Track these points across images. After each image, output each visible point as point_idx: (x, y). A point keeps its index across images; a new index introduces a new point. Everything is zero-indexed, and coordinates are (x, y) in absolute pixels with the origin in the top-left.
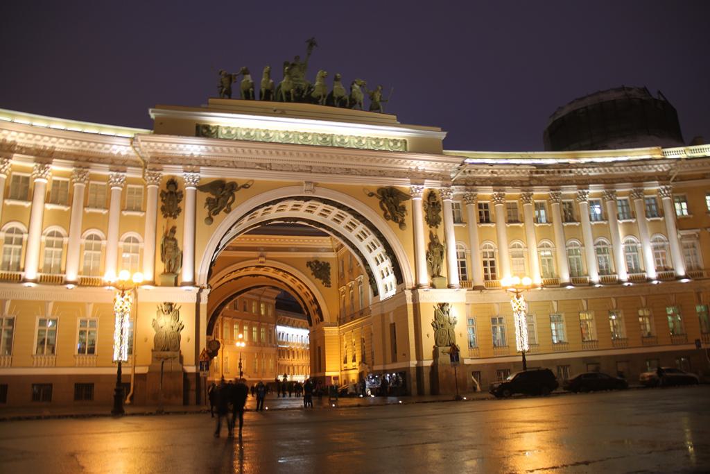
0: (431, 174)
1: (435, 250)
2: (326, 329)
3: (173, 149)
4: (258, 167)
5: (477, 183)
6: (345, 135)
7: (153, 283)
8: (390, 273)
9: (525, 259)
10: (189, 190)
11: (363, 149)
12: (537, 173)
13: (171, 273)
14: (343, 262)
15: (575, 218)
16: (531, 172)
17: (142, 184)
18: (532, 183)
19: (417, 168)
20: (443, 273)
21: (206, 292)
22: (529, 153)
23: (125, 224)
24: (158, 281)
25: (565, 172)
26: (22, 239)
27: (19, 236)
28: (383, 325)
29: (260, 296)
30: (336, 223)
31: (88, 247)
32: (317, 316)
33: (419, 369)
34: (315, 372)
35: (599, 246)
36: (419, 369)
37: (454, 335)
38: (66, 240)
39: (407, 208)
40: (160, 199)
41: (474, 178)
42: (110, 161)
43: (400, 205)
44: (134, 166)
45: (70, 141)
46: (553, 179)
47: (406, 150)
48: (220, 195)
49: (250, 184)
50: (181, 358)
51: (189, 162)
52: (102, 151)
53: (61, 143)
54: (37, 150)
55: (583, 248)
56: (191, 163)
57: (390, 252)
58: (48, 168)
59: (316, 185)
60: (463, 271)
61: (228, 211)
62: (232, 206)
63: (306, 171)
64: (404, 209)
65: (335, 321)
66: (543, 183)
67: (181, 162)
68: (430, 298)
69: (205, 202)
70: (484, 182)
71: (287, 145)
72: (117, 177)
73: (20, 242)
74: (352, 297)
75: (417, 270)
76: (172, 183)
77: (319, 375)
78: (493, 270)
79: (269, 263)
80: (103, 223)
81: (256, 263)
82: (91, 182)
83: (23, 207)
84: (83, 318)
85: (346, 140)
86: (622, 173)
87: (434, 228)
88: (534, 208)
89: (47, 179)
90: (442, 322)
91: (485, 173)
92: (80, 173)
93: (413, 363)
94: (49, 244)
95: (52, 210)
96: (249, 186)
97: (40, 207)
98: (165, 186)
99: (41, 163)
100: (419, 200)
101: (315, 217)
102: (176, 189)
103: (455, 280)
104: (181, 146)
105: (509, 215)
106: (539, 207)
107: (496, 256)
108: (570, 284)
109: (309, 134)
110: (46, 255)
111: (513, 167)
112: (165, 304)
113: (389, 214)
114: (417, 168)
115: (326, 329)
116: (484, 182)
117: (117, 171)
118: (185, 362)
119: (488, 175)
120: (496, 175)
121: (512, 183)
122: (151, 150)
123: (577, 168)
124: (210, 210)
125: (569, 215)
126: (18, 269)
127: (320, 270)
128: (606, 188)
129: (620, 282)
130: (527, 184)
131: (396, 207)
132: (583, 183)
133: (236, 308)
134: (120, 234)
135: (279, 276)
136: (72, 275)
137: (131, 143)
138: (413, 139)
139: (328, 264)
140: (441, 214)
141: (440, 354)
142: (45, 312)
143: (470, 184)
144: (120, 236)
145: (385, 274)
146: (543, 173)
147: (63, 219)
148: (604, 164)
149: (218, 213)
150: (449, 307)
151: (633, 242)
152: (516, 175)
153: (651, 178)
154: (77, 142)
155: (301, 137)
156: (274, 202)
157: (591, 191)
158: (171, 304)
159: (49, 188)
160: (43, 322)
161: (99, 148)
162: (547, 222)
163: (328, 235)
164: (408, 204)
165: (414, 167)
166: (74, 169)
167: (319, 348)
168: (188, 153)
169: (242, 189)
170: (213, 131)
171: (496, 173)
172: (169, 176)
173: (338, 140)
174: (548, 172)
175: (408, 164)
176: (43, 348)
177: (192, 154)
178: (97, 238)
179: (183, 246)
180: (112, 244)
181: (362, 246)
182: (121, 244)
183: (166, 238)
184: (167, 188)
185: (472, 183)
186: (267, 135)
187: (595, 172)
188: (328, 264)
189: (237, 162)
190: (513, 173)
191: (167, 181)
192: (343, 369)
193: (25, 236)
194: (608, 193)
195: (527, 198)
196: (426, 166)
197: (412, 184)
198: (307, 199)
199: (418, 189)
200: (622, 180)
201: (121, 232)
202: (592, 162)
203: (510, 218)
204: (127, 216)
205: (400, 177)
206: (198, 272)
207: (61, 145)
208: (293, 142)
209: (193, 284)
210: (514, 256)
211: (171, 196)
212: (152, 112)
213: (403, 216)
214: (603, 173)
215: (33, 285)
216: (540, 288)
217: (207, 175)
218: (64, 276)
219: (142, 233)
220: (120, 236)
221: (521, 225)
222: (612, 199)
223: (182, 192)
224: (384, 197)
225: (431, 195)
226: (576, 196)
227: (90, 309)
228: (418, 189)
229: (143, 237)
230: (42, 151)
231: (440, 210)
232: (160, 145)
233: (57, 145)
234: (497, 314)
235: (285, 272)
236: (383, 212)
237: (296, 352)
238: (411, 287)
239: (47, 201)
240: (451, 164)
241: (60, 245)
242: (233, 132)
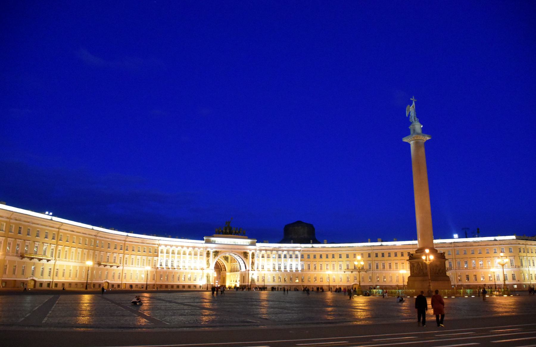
48: (216, 253)
56: (212, 248)
68: (251, 272)
70: (263, 250)
75: (249, 267)
76: (208, 251)
116: (263, 250)
121: (269, 250)
125: (280, 257)
132: (283, 251)
143: (261, 250)
200: (291, 251)
211: (208, 254)
217: (214, 250)
225: (253, 253)
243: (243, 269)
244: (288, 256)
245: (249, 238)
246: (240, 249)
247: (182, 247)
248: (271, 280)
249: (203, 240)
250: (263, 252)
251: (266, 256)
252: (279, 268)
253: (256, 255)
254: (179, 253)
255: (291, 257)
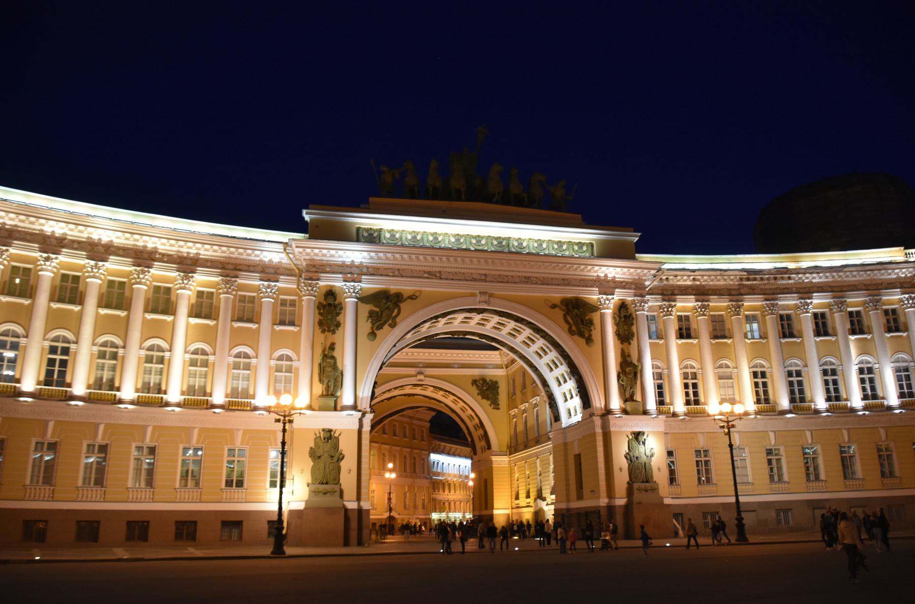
0: (622, 282)
1: (628, 370)
2: (494, 458)
3: (332, 256)
4: (426, 275)
5: (676, 292)
6: (523, 238)
7: (310, 408)
8: (574, 395)
9: (735, 381)
10: (350, 301)
11: (545, 255)
12: (748, 279)
13: (329, 397)
14: (514, 380)
15: (795, 333)
16: (741, 279)
17: (296, 294)
18: (742, 291)
19: (606, 276)
20: (638, 397)
21: (369, 417)
22: (738, 256)
23: (277, 341)
24: (315, 406)
25: (782, 278)
26: (163, 357)
27: (161, 354)
28: (566, 455)
29: (411, 418)
30: (511, 338)
31: (236, 366)
32: (483, 443)
33: (610, 508)
34: (480, 510)
35: (826, 367)
36: (610, 508)
37: (651, 469)
38: (211, 358)
39: (595, 322)
40: (317, 311)
41: (672, 286)
42: (260, 269)
43: (587, 318)
44: (288, 275)
45: (216, 248)
46: (767, 287)
47: (592, 254)
48: (384, 308)
49: (417, 294)
50: (341, 492)
51: (348, 270)
52: (253, 258)
53: (206, 250)
54: (180, 257)
55: (806, 369)
56: (351, 272)
57: (574, 371)
58: (192, 277)
59: (491, 295)
60: (661, 394)
61: (393, 326)
62: (398, 320)
63: (481, 280)
64: (591, 322)
65: (505, 449)
66: (756, 291)
67: (340, 270)
68: (623, 426)
69: (367, 314)
70: (685, 291)
71: (460, 251)
72: (269, 287)
73: (161, 360)
74: (526, 422)
76: (331, 293)
77: (484, 513)
78: (696, 394)
79: (428, 381)
80: (253, 339)
81: (413, 381)
82: (240, 293)
83: (165, 320)
84: (232, 447)
85: (525, 244)
86: (854, 279)
87: (626, 344)
88: (744, 321)
89: (190, 290)
90: (636, 454)
91: (685, 281)
92: (227, 282)
93: (603, 501)
94: (193, 363)
95: (197, 325)
96: (417, 297)
97: (183, 322)
98: (323, 297)
99: (184, 272)
100: (608, 312)
101: (488, 329)
102: (335, 300)
103: (651, 405)
104: (340, 252)
105: (714, 330)
106: (750, 319)
107: (699, 376)
108: (790, 412)
109: (483, 237)
110: (190, 375)
111: (719, 273)
112: (324, 430)
113: (574, 328)
114: (606, 276)
115: (494, 458)
116: (685, 291)
117: (269, 280)
118: (346, 496)
119: (689, 283)
120: (698, 283)
121: (718, 292)
122: (307, 257)
123: (798, 273)
124: (373, 324)
126: (159, 391)
127: (487, 389)
128: (834, 297)
129: (853, 410)
130: (737, 292)
131: (582, 321)
133: (384, 433)
134: (272, 351)
135: (439, 396)
136: (218, 398)
137: (285, 250)
138: (602, 243)
139: (496, 382)
140: (634, 328)
141: (636, 492)
142: (189, 440)
143: (669, 293)
144: (271, 355)
145: (568, 396)
146: (755, 279)
147: (209, 335)
148: (831, 269)
149: (382, 328)
150: (645, 437)
151: (869, 363)
152: (722, 283)
153: (891, 285)
154: (224, 249)
155: (474, 241)
156: (444, 315)
157: (815, 301)
158: (330, 431)
159: (193, 301)
160: (186, 450)
161: (249, 255)
162: (761, 337)
163: (497, 349)
164: (596, 317)
165: (602, 275)
166: (220, 278)
167: (486, 480)
168: (348, 260)
169: (409, 300)
170: (375, 235)
171: (699, 280)
172: (327, 286)
173: (516, 244)
174: (762, 279)
175: (596, 272)
176: (187, 480)
177: (353, 261)
178: (247, 356)
179: (343, 365)
180: (263, 364)
181: (541, 364)
182: (273, 363)
183: (325, 356)
184: (325, 299)
185: (670, 293)
186: (436, 238)
187: (820, 278)
188: (496, 382)
189: (403, 270)
190: (719, 280)
191: (324, 291)
192: (514, 506)
193: (167, 354)
194: (836, 304)
195: (737, 309)
196: (617, 273)
197: (600, 294)
198: (480, 311)
199: (607, 299)
200: (854, 287)
201: (273, 349)
202: (816, 267)
203: (715, 333)
204: (280, 330)
205: (587, 286)
206: (360, 394)
207: (206, 252)
208: (464, 247)
209: (355, 407)
210: (720, 378)
211: (329, 309)
212: (307, 213)
213: (591, 331)
214: (830, 279)
215: (177, 409)
216: (752, 417)
217: (368, 285)
218: (209, 398)
219: (297, 351)
220: (271, 355)
221: (729, 341)
222: (841, 311)
223: (341, 304)
224: (568, 309)
225: (622, 306)
226: (797, 307)
227: (239, 436)
228: (607, 299)
229: (298, 355)
230: (186, 258)
231: (633, 324)
232: (316, 251)
233: (202, 252)
234: (701, 446)
235: (446, 391)
236: (566, 327)
237: (452, 485)
238: (600, 413)
239: (190, 315)
240: (646, 271)
241: (205, 364)
242: (397, 236)
243: (571, 409)
244: (839, 322)
245: (588, 222)
246: (545, 282)
247: (143, 258)
248: (753, 468)
249: (298, 226)
250: (686, 304)
251: (701, 324)
252: (798, 395)
253: (643, 313)
254: (116, 296)
255: (857, 325)
